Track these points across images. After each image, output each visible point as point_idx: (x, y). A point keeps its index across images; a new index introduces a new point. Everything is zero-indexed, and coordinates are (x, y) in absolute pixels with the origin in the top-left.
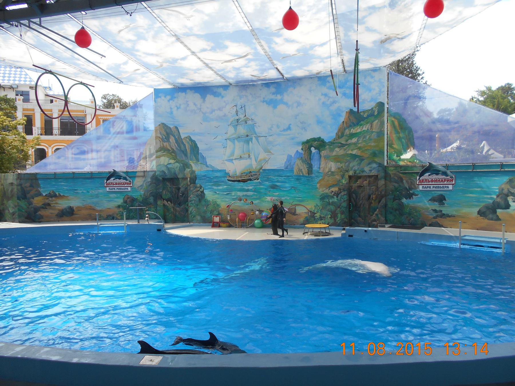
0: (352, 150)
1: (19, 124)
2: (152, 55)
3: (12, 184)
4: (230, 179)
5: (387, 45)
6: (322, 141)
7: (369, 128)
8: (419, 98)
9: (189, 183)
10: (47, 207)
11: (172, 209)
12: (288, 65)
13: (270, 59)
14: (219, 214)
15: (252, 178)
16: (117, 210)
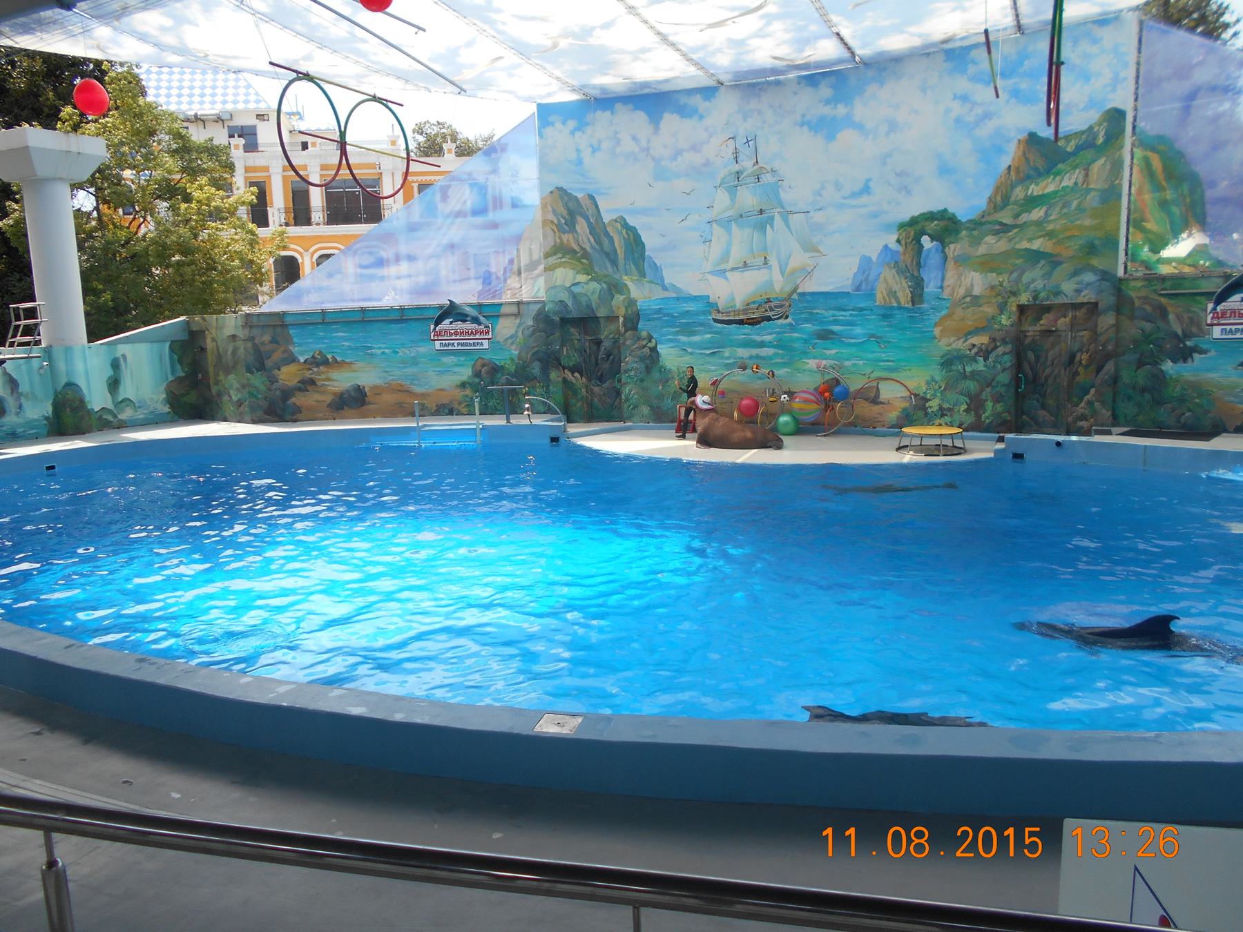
0: (1030, 240)
1: (243, 203)
2: (533, 18)
3: (234, 337)
4: (719, 317)
6: (950, 219)
9: (622, 330)
12: (867, 23)
15: (771, 314)
16: (459, 394)
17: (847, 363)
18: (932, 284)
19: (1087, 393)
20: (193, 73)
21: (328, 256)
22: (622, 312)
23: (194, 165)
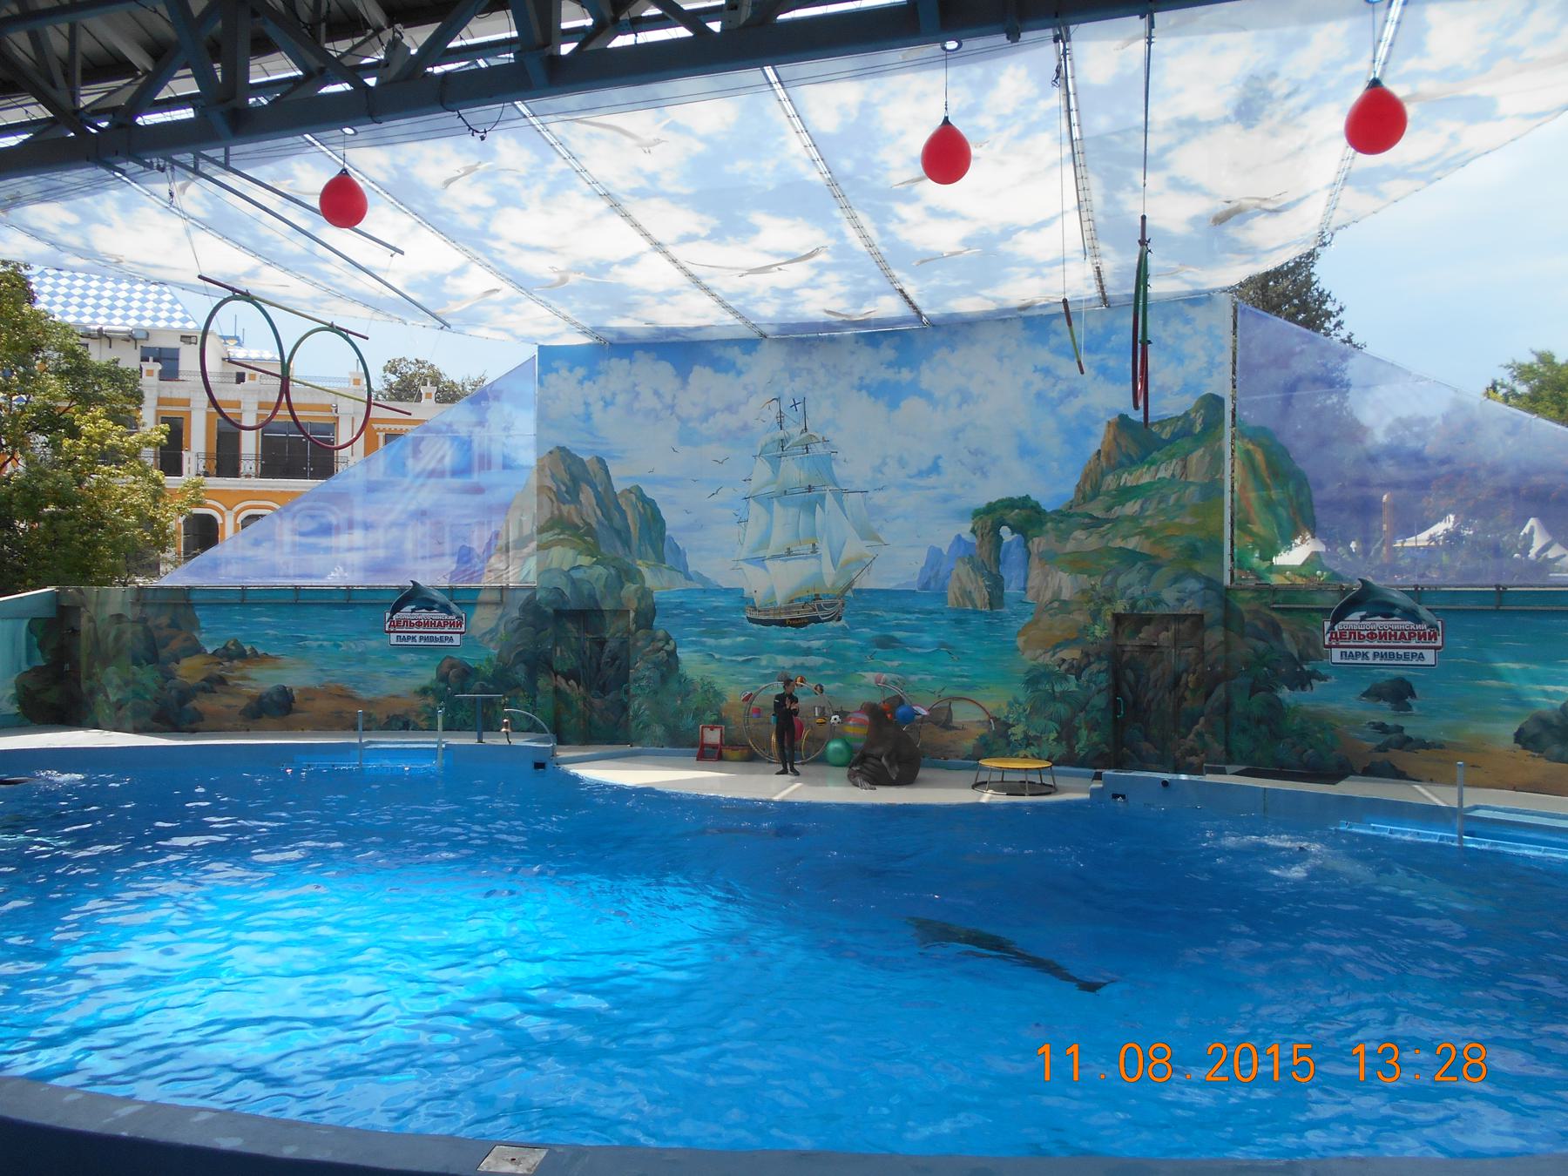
0: (1125, 538)
1: (149, 444)
2: (537, 249)
3: (119, 617)
4: (755, 615)
5: (1231, 230)
7: (1178, 472)
8: (1331, 382)
9: (633, 627)
10: (217, 688)
11: (580, 703)
12: (935, 282)
13: (883, 265)
14: (719, 722)
15: (820, 614)
16: (419, 702)
17: (913, 678)
18: (1013, 585)
19: (1197, 723)
20: (103, 280)
21: (256, 517)
22: (633, 605)
23: (89, 391)
